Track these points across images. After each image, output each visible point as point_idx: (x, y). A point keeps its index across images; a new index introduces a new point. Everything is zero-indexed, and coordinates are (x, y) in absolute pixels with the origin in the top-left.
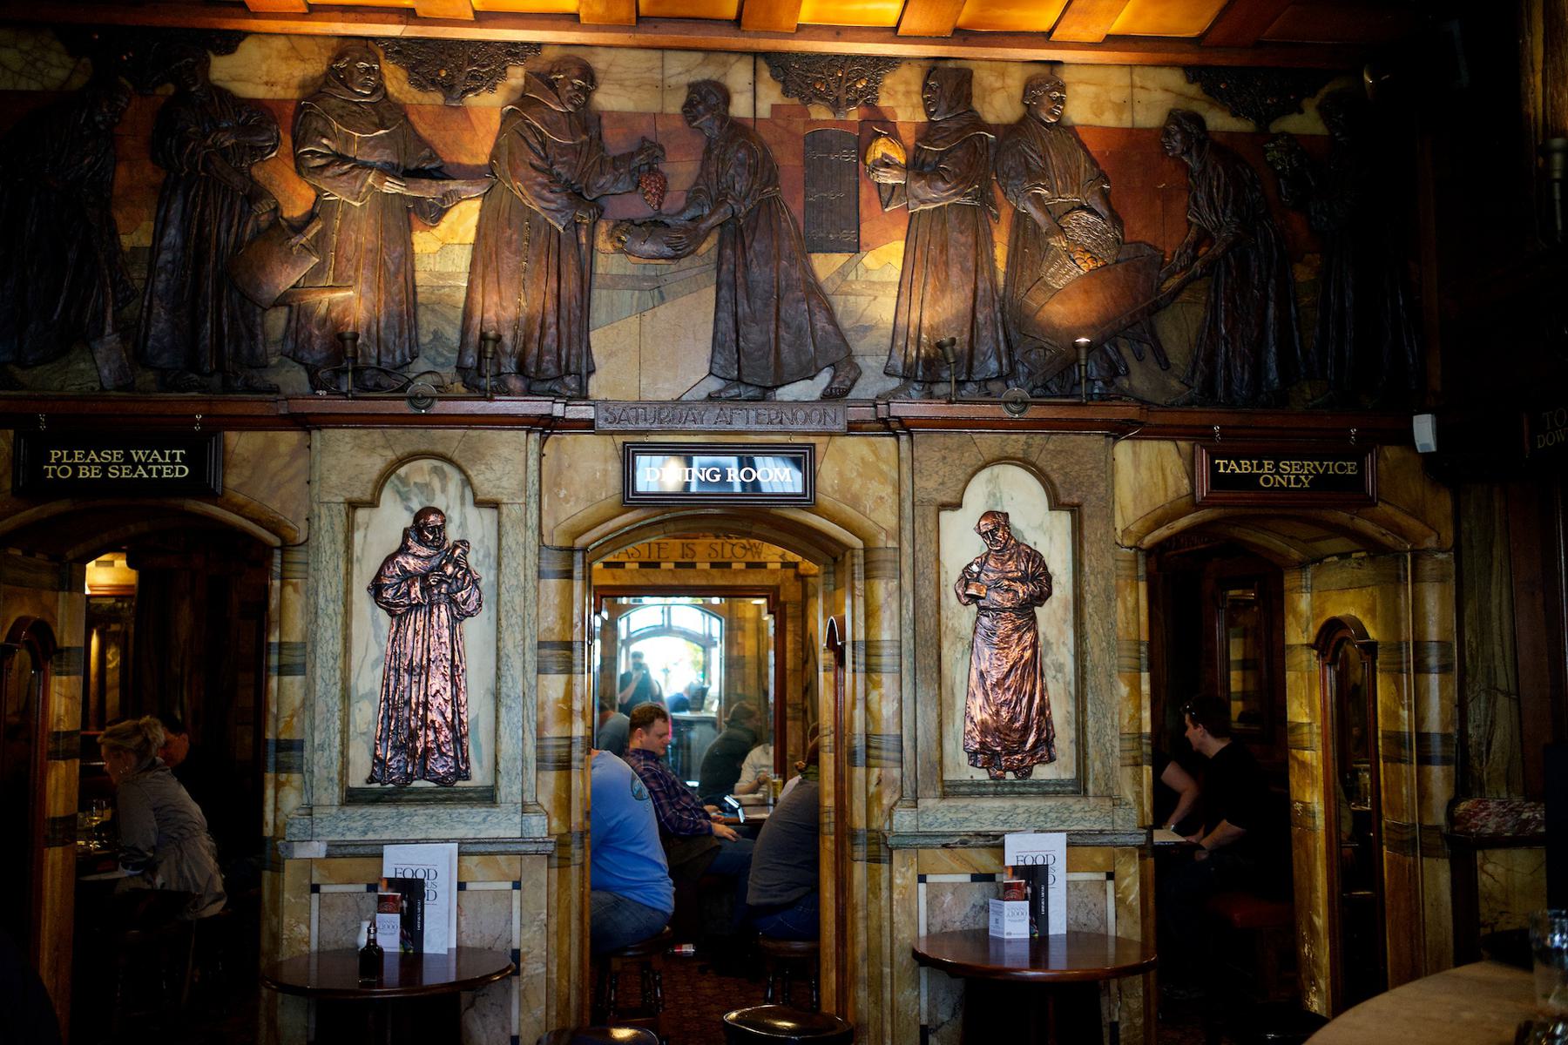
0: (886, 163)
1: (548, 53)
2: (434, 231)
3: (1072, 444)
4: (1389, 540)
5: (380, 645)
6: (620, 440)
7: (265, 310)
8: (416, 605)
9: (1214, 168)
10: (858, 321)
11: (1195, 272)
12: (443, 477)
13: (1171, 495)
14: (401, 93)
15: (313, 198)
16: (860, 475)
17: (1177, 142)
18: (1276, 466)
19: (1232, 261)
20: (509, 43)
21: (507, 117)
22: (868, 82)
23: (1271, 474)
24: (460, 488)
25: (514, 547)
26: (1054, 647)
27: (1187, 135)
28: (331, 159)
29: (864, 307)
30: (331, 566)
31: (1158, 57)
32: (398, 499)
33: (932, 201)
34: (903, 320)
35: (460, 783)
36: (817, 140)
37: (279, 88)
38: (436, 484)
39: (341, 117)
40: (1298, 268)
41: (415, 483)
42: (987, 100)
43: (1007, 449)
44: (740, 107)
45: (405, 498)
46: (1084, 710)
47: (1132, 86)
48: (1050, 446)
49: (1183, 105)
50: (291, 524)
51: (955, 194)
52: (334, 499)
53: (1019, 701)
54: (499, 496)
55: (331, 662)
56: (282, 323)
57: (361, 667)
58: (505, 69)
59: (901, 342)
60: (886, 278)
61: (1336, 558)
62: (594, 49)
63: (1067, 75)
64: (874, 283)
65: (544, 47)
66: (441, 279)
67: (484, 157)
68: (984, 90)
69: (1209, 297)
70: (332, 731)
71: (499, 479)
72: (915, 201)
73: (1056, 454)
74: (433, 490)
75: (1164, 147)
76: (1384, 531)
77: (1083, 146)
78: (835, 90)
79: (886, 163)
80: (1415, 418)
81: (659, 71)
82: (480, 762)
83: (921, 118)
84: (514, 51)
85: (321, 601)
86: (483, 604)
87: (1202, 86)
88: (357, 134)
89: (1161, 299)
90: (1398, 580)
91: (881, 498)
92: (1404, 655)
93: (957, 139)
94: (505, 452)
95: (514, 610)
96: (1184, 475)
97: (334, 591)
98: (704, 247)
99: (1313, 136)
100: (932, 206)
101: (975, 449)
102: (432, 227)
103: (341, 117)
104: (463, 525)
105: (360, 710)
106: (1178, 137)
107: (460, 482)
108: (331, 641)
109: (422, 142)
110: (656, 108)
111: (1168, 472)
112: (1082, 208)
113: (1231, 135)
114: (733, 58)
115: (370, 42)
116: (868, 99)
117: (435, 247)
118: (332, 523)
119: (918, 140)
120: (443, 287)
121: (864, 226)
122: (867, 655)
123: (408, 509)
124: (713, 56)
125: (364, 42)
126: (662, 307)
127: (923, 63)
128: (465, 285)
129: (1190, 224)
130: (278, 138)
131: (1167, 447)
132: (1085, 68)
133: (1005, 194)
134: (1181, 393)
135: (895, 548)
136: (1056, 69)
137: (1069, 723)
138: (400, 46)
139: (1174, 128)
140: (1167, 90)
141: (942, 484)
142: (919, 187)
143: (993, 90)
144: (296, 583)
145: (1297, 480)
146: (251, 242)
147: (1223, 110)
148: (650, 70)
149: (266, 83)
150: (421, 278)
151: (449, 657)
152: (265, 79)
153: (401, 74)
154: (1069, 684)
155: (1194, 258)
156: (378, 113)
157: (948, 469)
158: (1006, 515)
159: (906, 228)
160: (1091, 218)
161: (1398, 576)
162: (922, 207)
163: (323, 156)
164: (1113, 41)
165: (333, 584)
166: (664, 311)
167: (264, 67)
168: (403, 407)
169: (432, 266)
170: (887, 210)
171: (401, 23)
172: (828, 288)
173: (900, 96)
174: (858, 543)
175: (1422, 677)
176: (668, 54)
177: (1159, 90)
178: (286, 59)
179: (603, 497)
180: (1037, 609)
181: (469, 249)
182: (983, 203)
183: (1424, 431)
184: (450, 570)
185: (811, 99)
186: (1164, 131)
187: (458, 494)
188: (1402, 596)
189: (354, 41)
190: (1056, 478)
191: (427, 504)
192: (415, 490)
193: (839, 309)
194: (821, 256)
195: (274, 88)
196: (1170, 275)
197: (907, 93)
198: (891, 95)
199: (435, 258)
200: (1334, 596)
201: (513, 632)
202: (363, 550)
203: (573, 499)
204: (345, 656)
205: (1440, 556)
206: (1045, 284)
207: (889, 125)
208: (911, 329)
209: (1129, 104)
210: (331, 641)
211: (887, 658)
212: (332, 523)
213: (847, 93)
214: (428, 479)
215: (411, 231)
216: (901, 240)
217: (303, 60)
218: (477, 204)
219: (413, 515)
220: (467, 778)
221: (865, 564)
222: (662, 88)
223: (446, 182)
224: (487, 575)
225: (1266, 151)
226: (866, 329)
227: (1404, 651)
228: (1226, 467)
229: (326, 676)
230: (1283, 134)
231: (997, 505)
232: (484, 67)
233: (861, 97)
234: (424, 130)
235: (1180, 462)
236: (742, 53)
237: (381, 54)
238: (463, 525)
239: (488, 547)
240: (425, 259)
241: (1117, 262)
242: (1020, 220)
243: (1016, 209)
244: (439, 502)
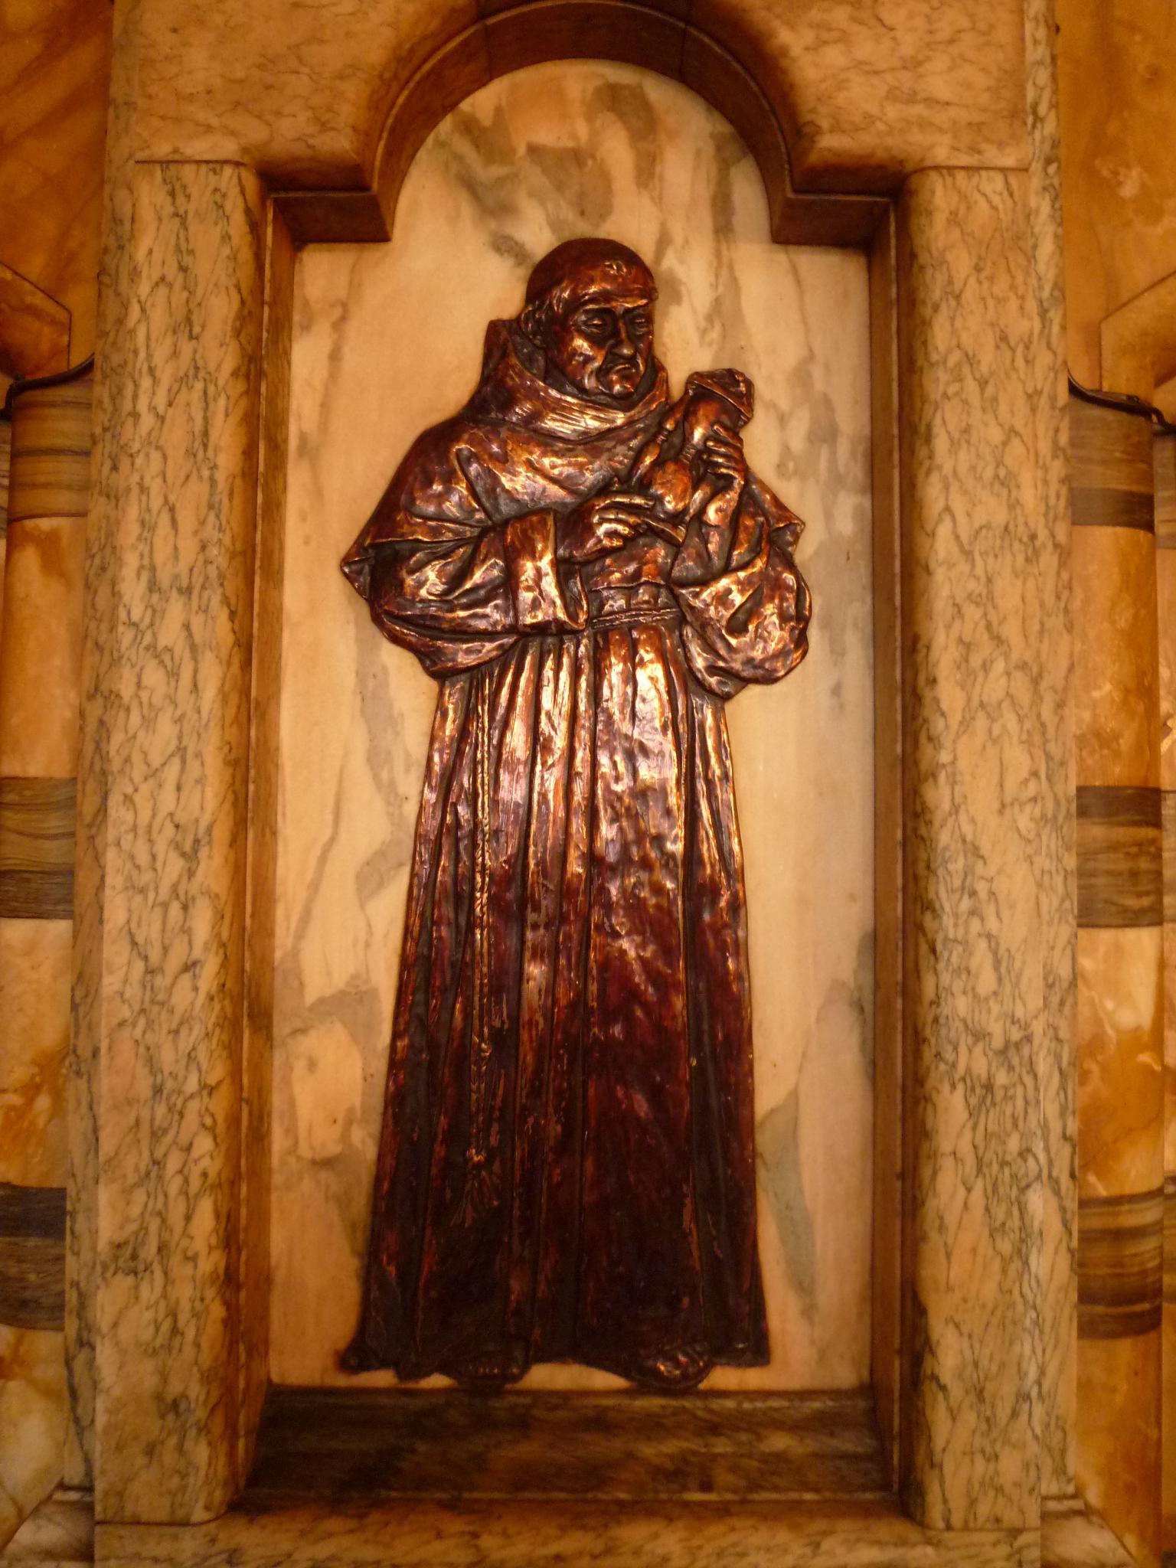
5: (390, 792)
25: (987, 358)
30: (176, 438)
32: (467, 210)
35: (724, 1377)
41: (534, 150)
50: (38, 300)
52: (198, 147)
55: (174, 866)
57: (315, 887)
70: (174, 1187)
71: (913, 64)
74: (605, 177)
82: (803, 1286)
85: (133, 590)
86: (814, 634)
95: (998, 640)
97: (188, 547)
105: (312, 1065)
107: (709, 149)
118: (183, 252)
123: (504, 246)
144: (53, 538)
151: (676, 847)
165: (187, 519)
187: (705, 192)
191: (584, 229)
192: (534, 175)
202: (325, 406)
204: (237, 839)
212: (183, 252)
214: (582, 130)
219: (524, 272)
220: (759, 1352)
224: (828, 516)
229: (150, 931)
239: (827, 402)
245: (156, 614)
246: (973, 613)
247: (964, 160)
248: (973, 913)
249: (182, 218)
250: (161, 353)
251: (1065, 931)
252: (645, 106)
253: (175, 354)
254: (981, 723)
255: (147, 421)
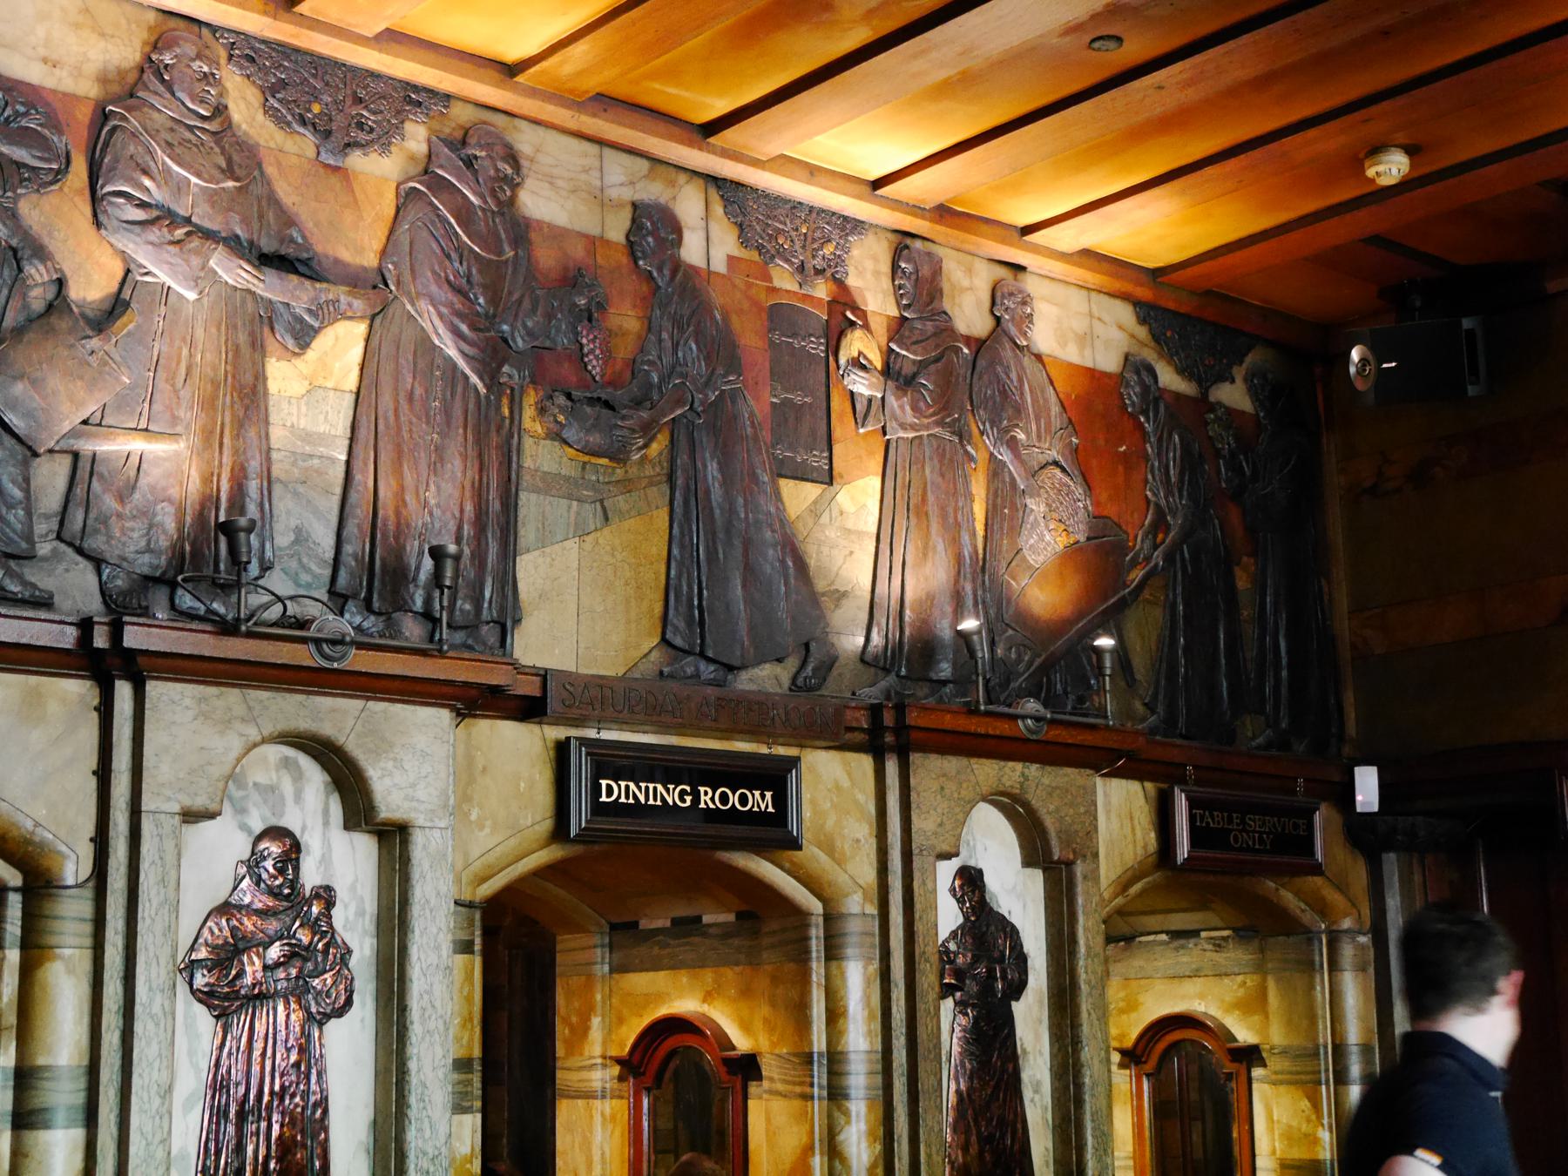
0: (858, 364)
1: (462, 114)
2: (297, 362)
3: (1066, 779)
4: (1308, 917)
5: (195, 1066)
6: (560, 733)
7: (36, 455)
8: (257, 997)
9: (1170, 436)
10: (833, 583)
11: (1156, 565)
12: (298, 777)
13: (1140, 851)
14: (252, 126)
15: (119, 274)
16: (834, 806)
17: (1132, 396)
18: (1243, 822)
19: (1187, 555)
20: (408, 84)
21: (406, 198)
22: (836, 248)
23: (1240, 831)
24: (322, 796)
26: (1031, 1057)
27: (1145, 389)
28: (155, 213)
29: (840, 563)
31: (1117, 285)
33: (913, 427)
34: (882, 587)
36: (780, 317)
37: (64, 74)
38: (287, 787)
39: (169, 144)
40: (1238, 572)
41: (255, 784)
42: (957, 301)
43: (1004, 780)
44: (692, 251)
45: (241, 811)
46: (1081, 1148)
47: (1091, 315)
48: (1046, 781)
49: (1135, 349)
51: (940, 423)
53: (1003, 1137)
54: (413, 815)
56: (61, 483)
58: (402, 122)
59: (880, 618)
60: (861, 527)
61: (1164, 937)
62: (517, 122)
63: (1031, 284)
64: (849, 531)
65: (453, 102)
66: (309, 443)
67: (372, 255)
68: (953, 287)
69: (1167, 596)
71: (413, 786)
72: (894, 424)
73: (1052, 789)
74: (282, 798)
75: (1123, 399)
76: (1303, 906)
77: (1052, 383)
78: (800, 250)
79: (858, 364)
80: (1357, 769)
81: (598, 174)
83: (894, 312)
84: (414, 98)
87: (1150, 330)
88: (194, 180)
89: (1130, 593)
90: (1309, 967)
91: (858, 841)
92: (1322, 1063)
93: (937, 346)
94: (421, 741)
95: (433, 1006)
96: (1151, 827)
97: (163, 972)
98: (655, 448)
99: (1243, 413)
100: (911, 435)
101: (972, 778)
102: (295, 354)
103: (169, 144)
104: (326, 860)
106: (1137, 389)
107: (322, 788)
108: (156, 1064)
109: (289, 221)
110: (595, 231)
111: (1136, 822)
112: (1056, 463)
113: (1178, 396)
114: (682, 178)
115: (205, 31)
116: (833, 272)
117: (299, 388)
119: (890, 340)
120: (311, 456)
121: (837, 449)
122: (830, 1073)
123: (244, 827)
124: (661, 169)
125: (196, 29)
126: (606, 531)
127: (889, 235)
128: (343, 457)
129: (1148, 501)
130: (68, 162)
131: (1134, 787)
132: (1047, 282)
133: (982, 433)
134: (1144, 720)
135: (873, 916)
136: (1021, 276)
137: (1047, 1166)
138: (252, 48)
139: (1132, 377)
140: (1120, 327)
141: (941, 825)
142: (899, 405)
143: (963, 290)
145: (1261, 841)
146: (19, 332)
147: (1169, 363)
148: (586, 171)
149: (45, 61)
150: (278, 435)
152: (42, 52)
153: (253, 95)
154: (1046, 1108)
155: (1155, 547)
156: (223, 153)
157: (945, 805)
158: (980, 872)
159: (881, 460)
160: (1066, 479)
161: (1312, 963)
162: (902, 434)
163: (143, 205)
164: (1088, 256)
166: (606, 536)
167: (41, 32)
168: (303, 655)
169: (294, 419)
170: (862, 431)
171: (265, 13)
172: (801, 530)
173: (869, 276)
174: (816, 906)
175: (1341, 1088)
176: (607, 152)
177: (1115, 327)
178: (77, 26)
179: (529, 822)
180: (1014, 1004)
181: (349, 400)
182: (961, 438)
183: (1367, 788)
184: (304, 937)
185: (773, 257)
186: (1119, 379)
187: (320, 807)
188: (1318, 988)
189: (181, 24)
190: (1049, 823)
193: (812, 562)
194: (791, 483)
195: (57, 71)
196: (1134, 563)
197: (877, 273)
198: (861, 274)
199: (299, 409)
200: (1160, 986)
201: (432, 1044)
203: (488, 823)
205: (1363, 939)
206: (1024, 559)
207: (860, 313)
208: (892, 603)
209: (1085, 339)
210: (156, 1064)
211: (859, 1079)
213: (814, 257)
215: (264, 356)
216: (877, 475)
217: (103, 35)
218: (361, 328)
221: (825, 938)
222: (601, 200)
223: (325, 285)
224: (362, 948)
225: (1206, 423)
226: (840, 596)
227: (1322, 1057)
228: (1202, 817)
229: (148, 1128)
230: (1220, 404)
231: (971, 857)
232: (374, 113)
233: (830, 266)
234: (286, 193)
235: (1146, 808)
236: (695, 173)
237: (223, 54)
238: (326, 860)
239: (362, 899)
240: (285, 405)
241: (1088, 539)
242: (996, 469)
243: (992, 454)
244: (291, 821)
245: (151, 1001)
246: (426, 997)
247: (429, 824)
248: (424, 1108)
249: (161, 837)
250: (153, 892)
251: (448, 1115)
252: (298, 767)
253: (159, 893)
254: (428, 1038)
255: (148, 921)
